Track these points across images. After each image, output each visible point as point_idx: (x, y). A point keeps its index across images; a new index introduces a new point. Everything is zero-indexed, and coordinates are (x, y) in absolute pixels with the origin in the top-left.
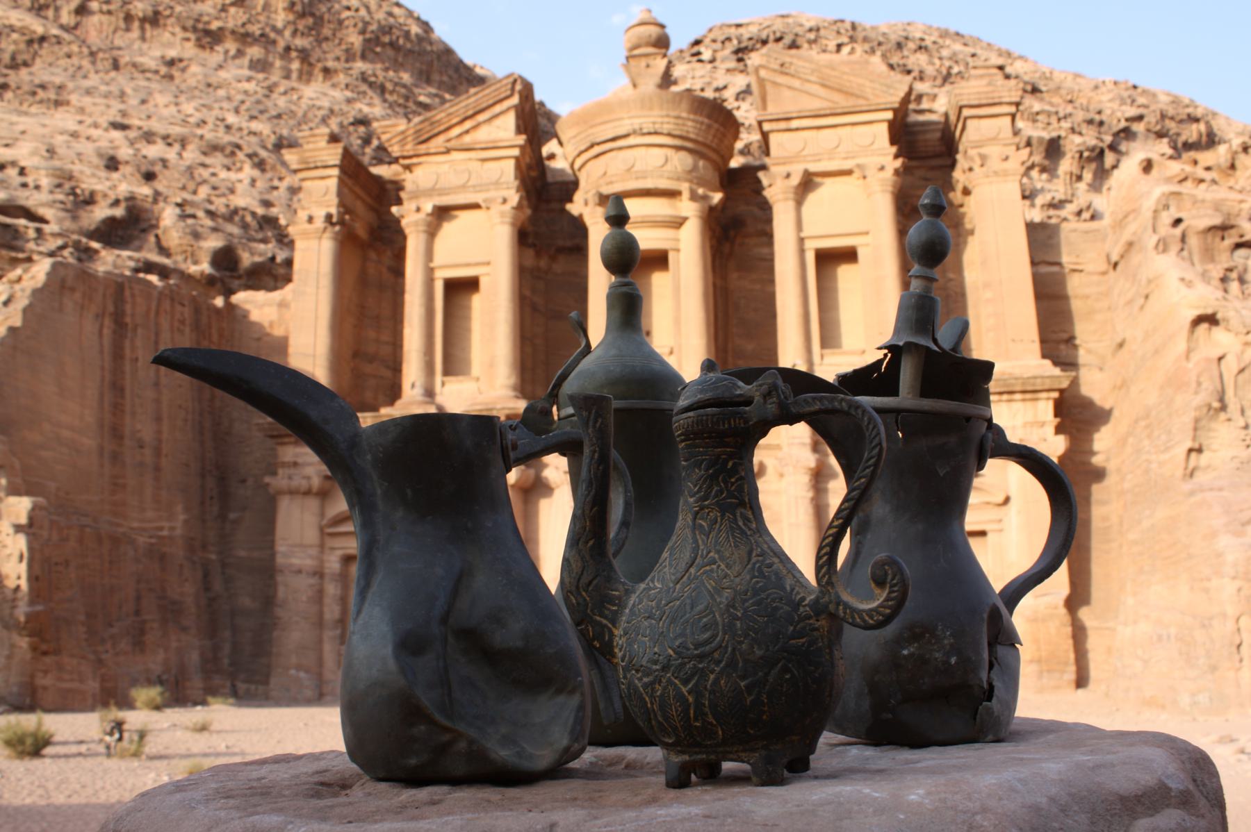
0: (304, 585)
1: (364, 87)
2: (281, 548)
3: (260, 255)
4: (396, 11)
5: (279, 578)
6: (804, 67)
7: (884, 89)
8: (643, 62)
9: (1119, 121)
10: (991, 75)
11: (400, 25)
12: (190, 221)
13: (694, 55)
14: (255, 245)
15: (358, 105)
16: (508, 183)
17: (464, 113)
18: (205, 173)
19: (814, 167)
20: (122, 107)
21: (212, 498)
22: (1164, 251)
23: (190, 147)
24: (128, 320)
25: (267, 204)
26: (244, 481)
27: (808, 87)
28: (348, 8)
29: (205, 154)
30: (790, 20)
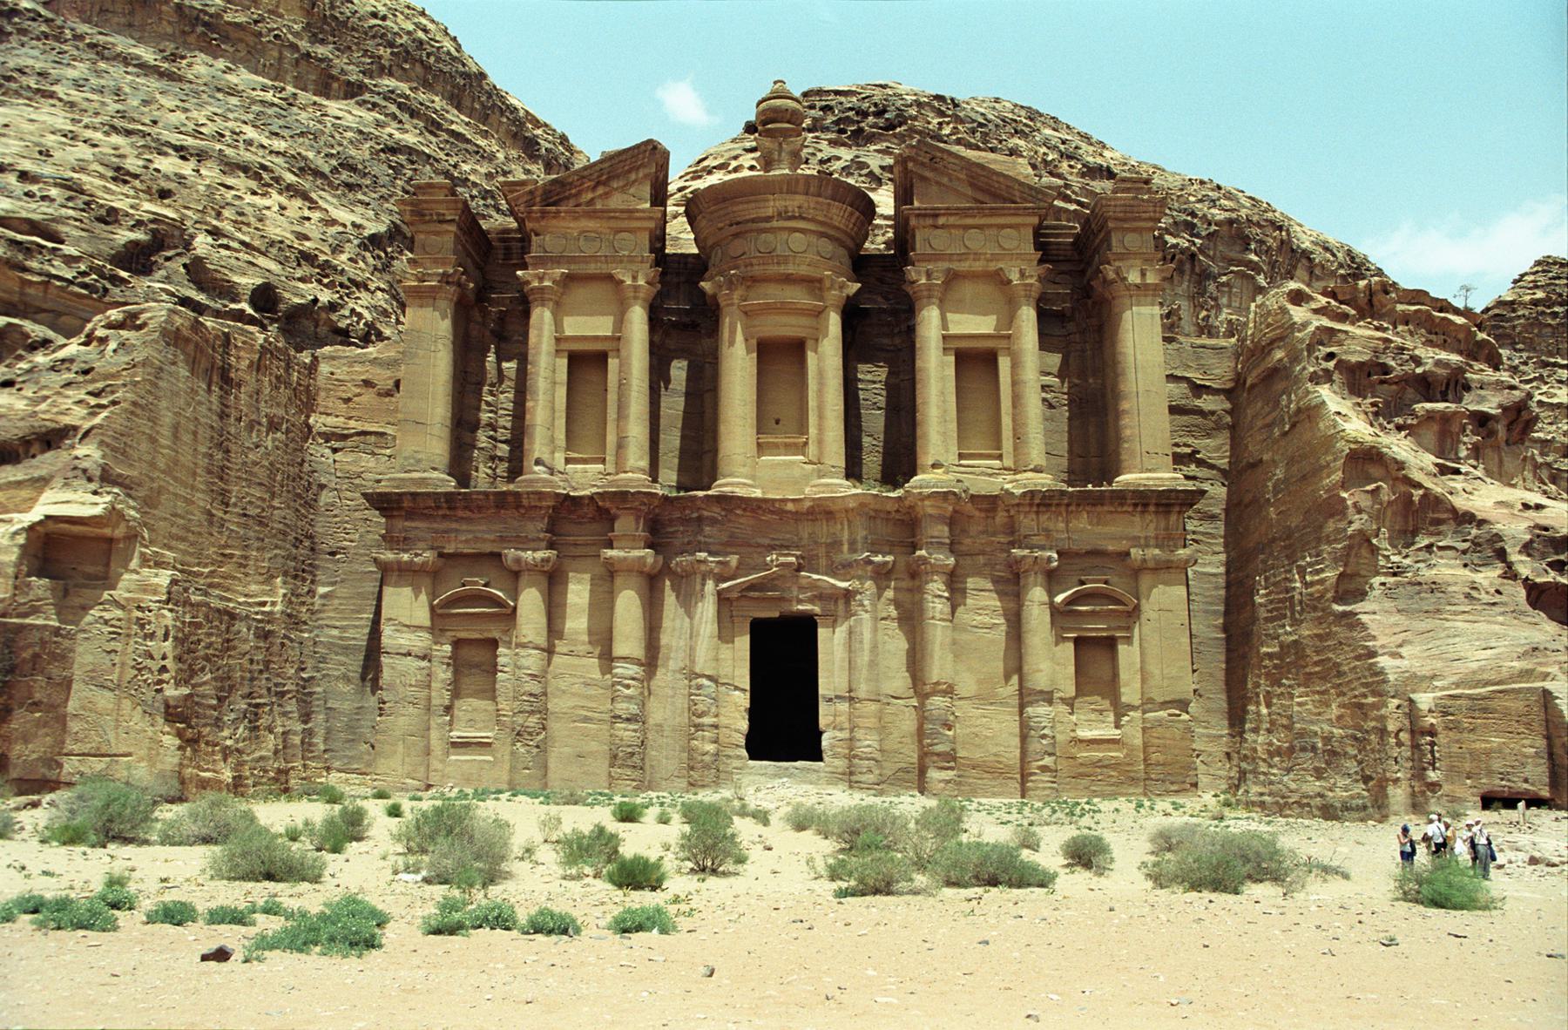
1: (393, 108)
3: (303, 296)
4: (423, 21)
5: (385, 660)
9: (1210, 224)
14: (294, 283)
15: (388, 130)
17: (599, 177)
19: (955, 266)
20: (119, 107)
21: (304, 571)
22: (1317, 384)
23: (209, 164)
24: (232, 375)
26: (333, 554)
28: (375, 15)
29: (224, 173)
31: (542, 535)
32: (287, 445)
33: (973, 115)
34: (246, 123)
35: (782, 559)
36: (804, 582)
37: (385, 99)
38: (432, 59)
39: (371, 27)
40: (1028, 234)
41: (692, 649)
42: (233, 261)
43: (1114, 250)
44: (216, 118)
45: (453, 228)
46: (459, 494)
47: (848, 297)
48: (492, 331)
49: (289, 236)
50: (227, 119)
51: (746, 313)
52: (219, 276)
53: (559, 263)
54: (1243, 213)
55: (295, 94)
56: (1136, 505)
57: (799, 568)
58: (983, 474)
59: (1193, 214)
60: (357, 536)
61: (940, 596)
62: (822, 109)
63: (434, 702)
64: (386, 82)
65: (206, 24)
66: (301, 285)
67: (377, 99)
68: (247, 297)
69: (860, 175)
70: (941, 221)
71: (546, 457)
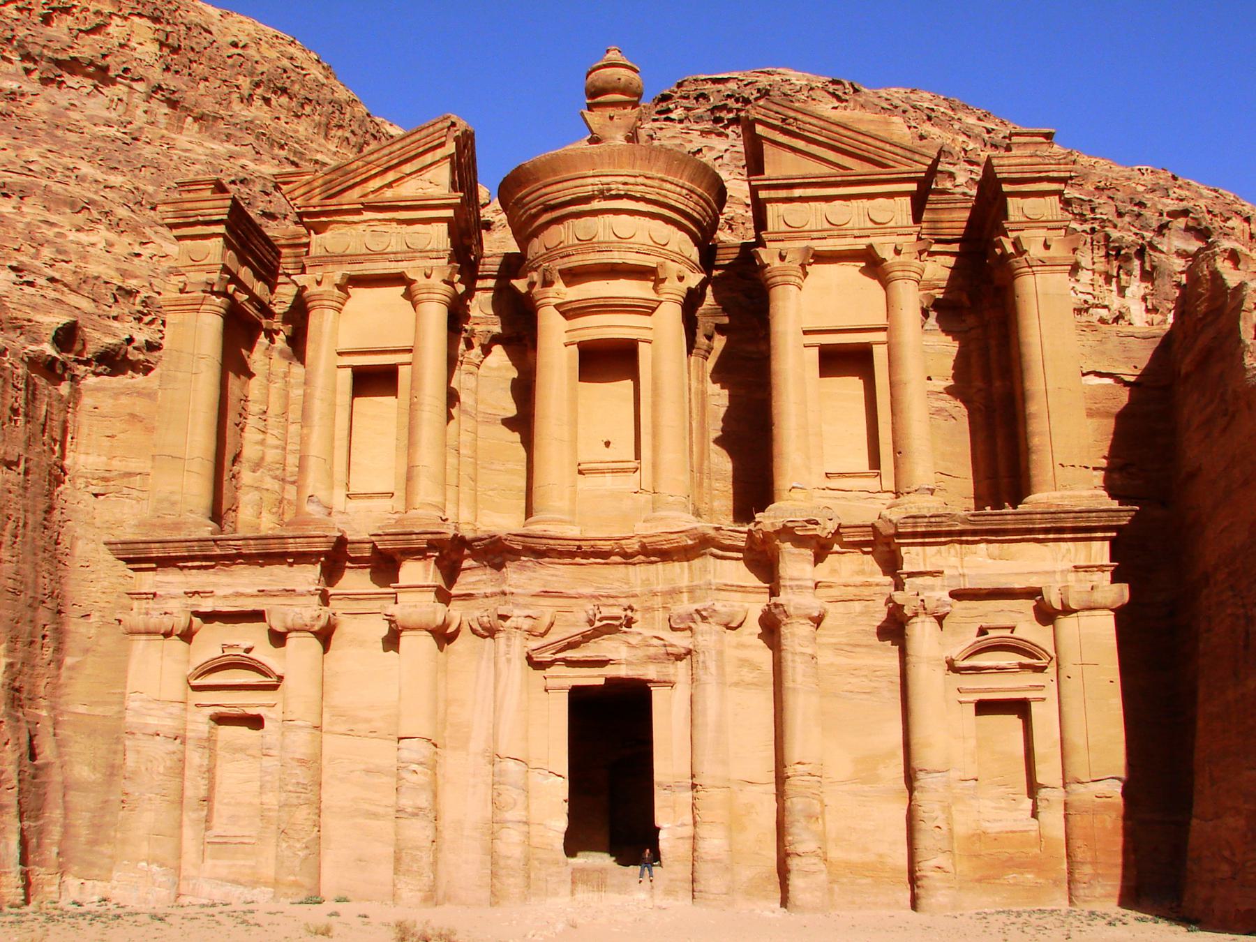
0: (161, 749)
1: (251, 139)
2: (133, 704)
6: (810, 124)
7: (909, 154)
8: (610, 111)
9: (1161, 215)
10: (1036, 143)
11: (297, 67)
12: (28, 289)
13: (659, 113)
16: (438, 251)
18: (50, 233)
21: (44, 637)
25: (124, 274)
27: (813, 149)
28: (235, 45)
30: (777, 78)
31: (313, 588)
32: (26, 489)
33: (876, 101)
34: (82, 158)
35: (606, 612)
36: (634, 640)
37: (241, 129)
38: (297, 87)
39: (229, 57)
40: (906, 202)
41: (495, 726)
42: (39, 300)
43: (1011, 219)
44: (49, 155)
45: (221, 229)
46: (215, 541)
47: (689, 289)
48: (281, 352)
49: (113, 273)
50: (61, 155)
51: (564, 314)
52: (19, 315)
53: (341, 263)
54: (1202, 203)
55: (140, 128)
56: (1046, 531)
57: (629, 622)
58: (858, 498)
59: (1141, 204)
60: (115, 595)
61: (803, 654)
62: (697, 99)
63: (189, 793)
64: (245, 113)
65: (51, 60)
66: (116, 324)
67: (232, 131)
68: (50, 338)
69: (738, 167)
70: (797, 193)
71: (322, 494)
